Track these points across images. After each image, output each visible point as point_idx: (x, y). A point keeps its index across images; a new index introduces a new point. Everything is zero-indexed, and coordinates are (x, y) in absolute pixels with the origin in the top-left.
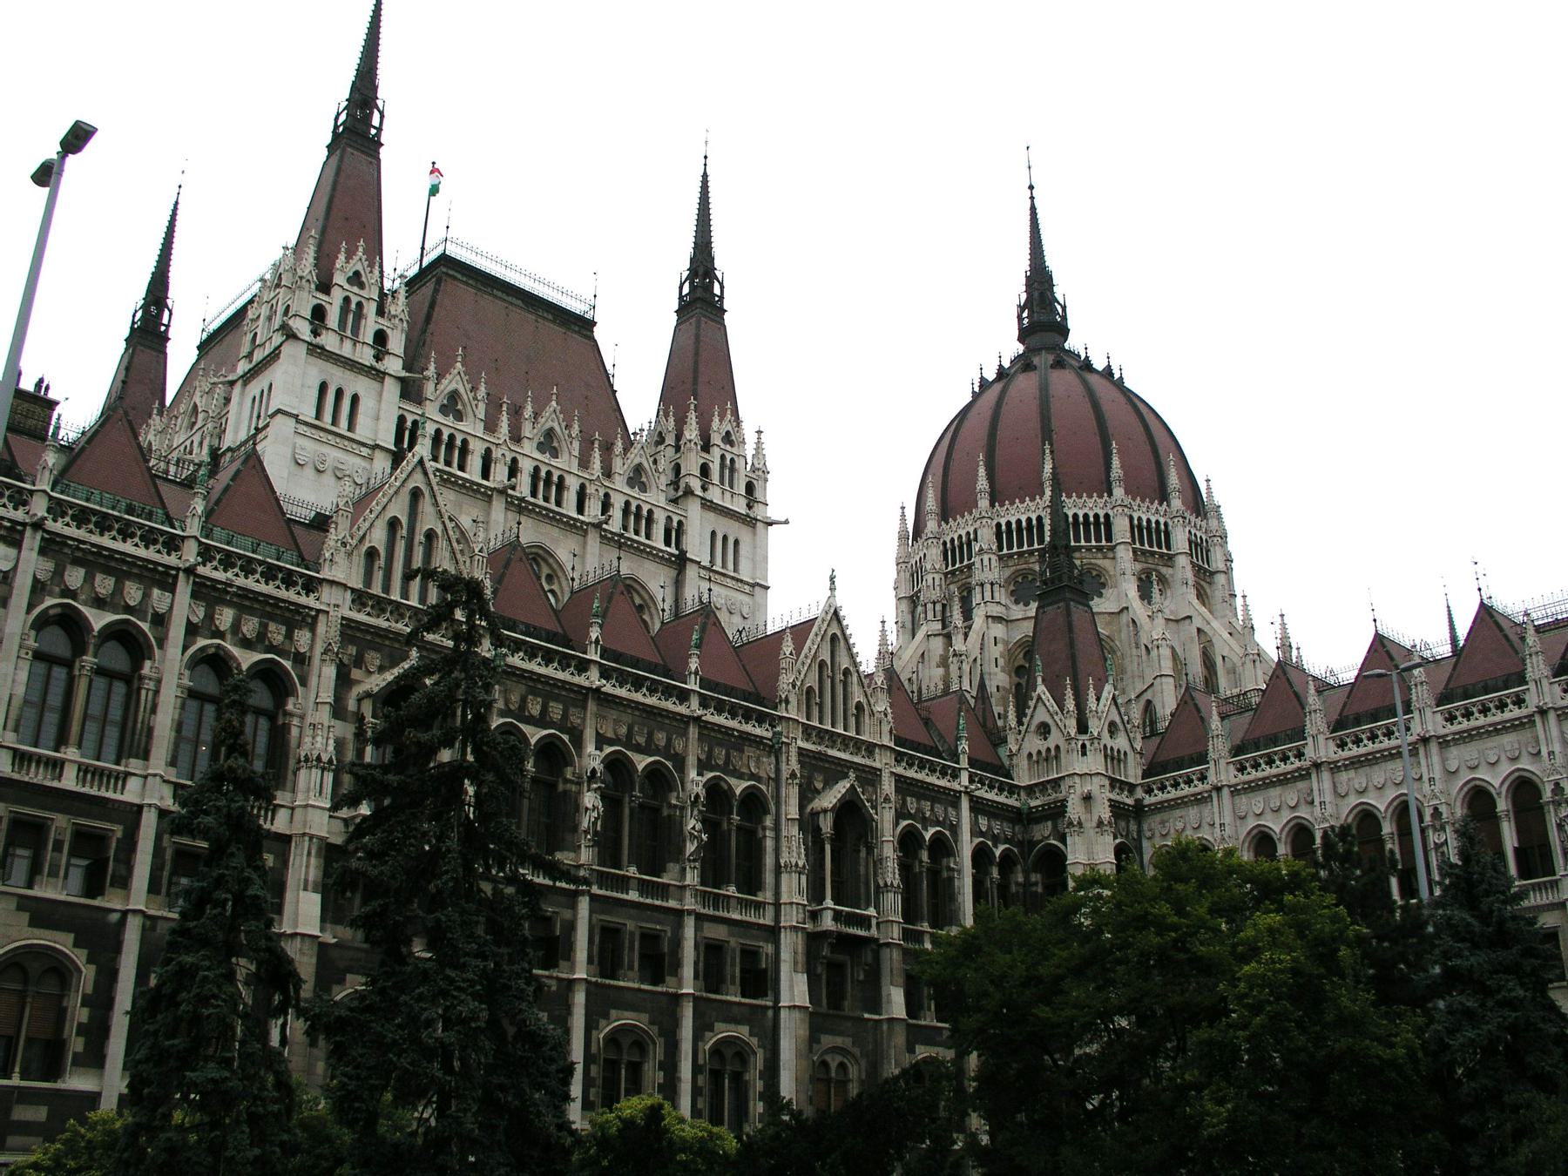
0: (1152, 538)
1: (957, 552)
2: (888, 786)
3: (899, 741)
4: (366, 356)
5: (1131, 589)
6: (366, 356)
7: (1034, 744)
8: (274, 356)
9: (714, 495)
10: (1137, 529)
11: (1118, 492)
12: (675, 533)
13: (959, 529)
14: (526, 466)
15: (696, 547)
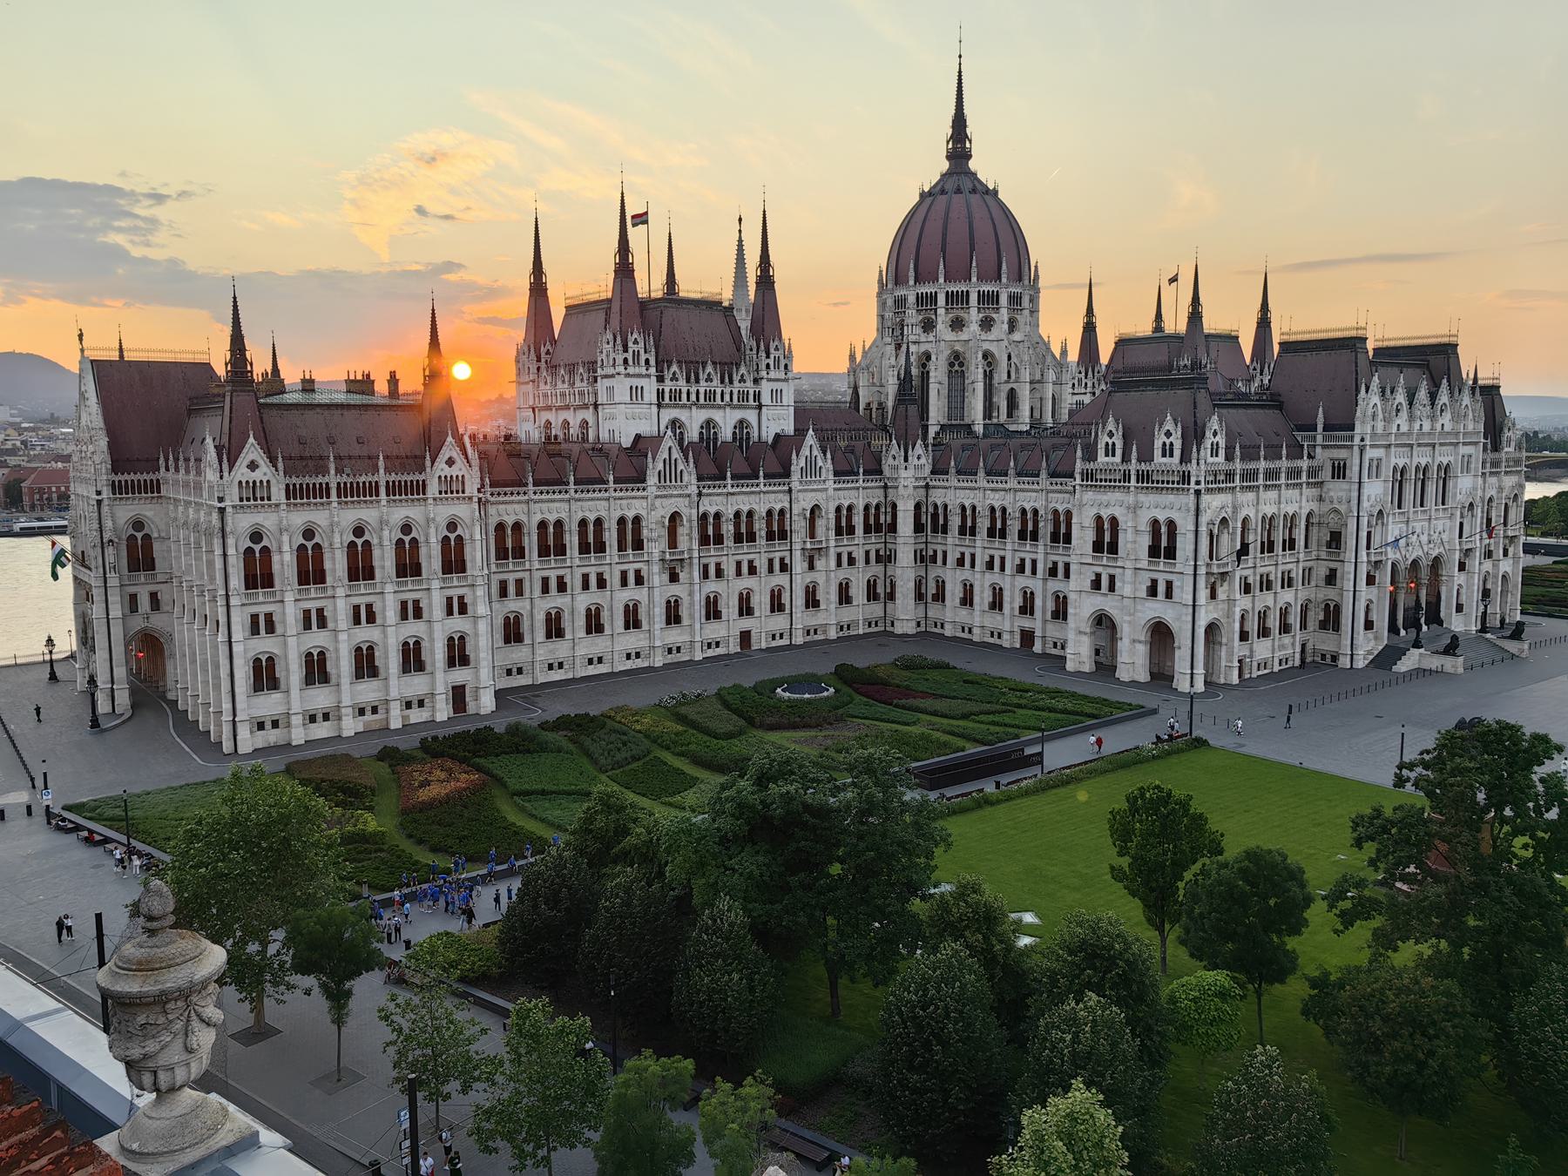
0: (989, 300)
1: (900, 303)
2: (831, 492)
3: (836, 474)
4: (643, 371)
5: (974, 328)
6: (643, 371)
7: (891, 461)
8: (612, 376)
9: (772, 375)
10: (982, 297)
11: (974, 279)
12: (757, 396)
13: (900, 292)
14: (702, 391)
15: (766, 399)
